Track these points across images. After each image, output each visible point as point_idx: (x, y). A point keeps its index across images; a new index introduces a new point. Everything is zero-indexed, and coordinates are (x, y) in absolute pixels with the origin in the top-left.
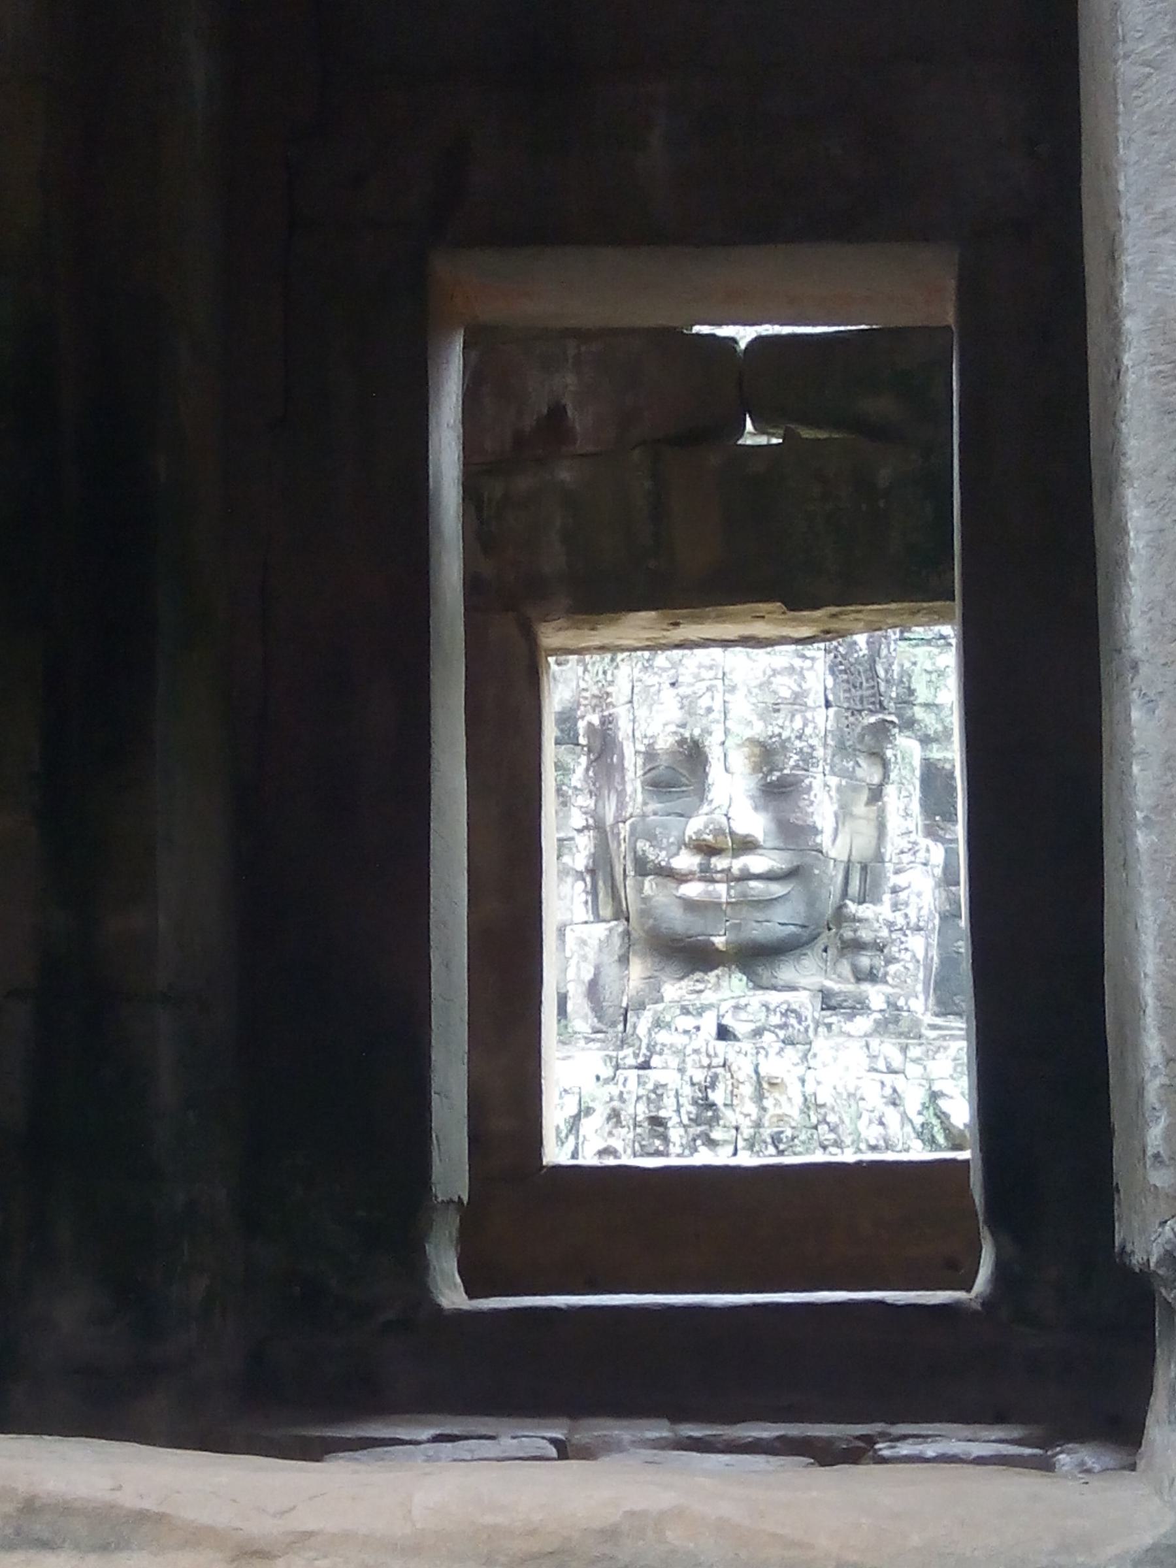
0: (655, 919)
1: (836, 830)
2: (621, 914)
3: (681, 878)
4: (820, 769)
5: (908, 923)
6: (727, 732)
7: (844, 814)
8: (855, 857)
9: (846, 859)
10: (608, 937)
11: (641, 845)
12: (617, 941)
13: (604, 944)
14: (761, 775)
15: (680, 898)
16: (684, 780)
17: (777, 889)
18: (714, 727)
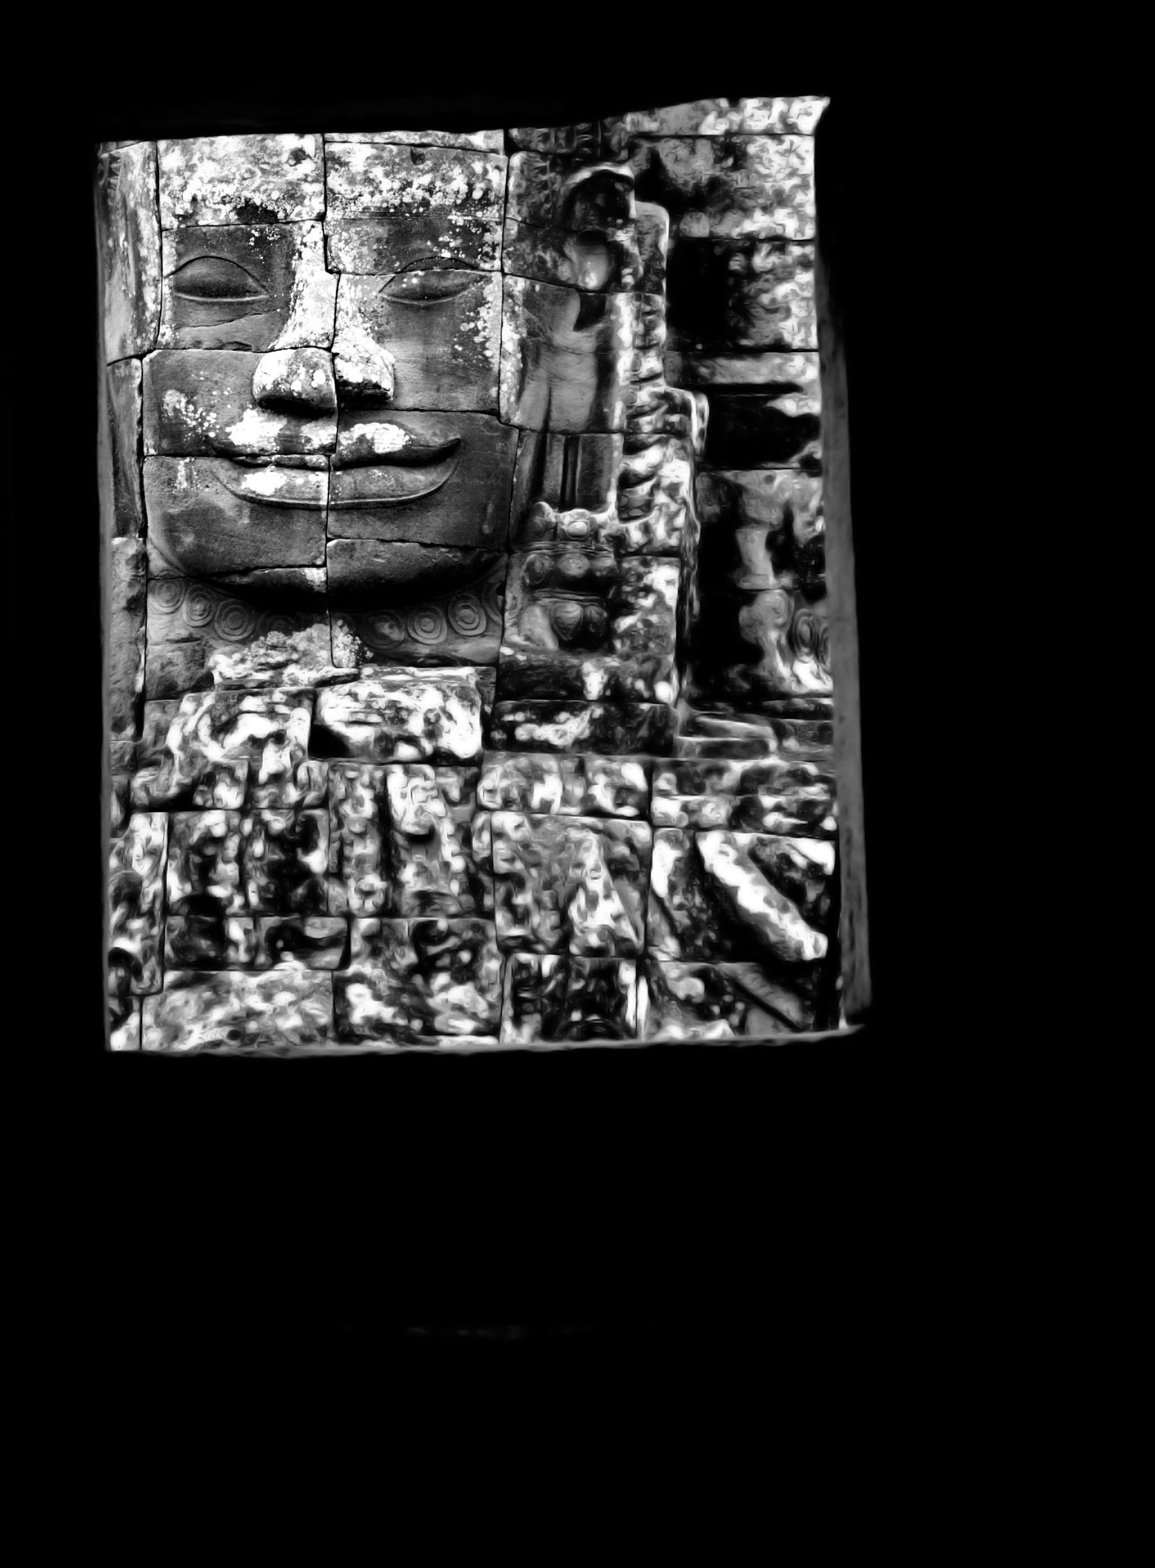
1: (523, 375)
3: (249, 461)
4: (497, 264)
6: (329, 196)
8: (557, 422)
9: (537, 423)
11: (173, 399)
15: (244, 498)
17: (419, 481)
18: (307, 188)
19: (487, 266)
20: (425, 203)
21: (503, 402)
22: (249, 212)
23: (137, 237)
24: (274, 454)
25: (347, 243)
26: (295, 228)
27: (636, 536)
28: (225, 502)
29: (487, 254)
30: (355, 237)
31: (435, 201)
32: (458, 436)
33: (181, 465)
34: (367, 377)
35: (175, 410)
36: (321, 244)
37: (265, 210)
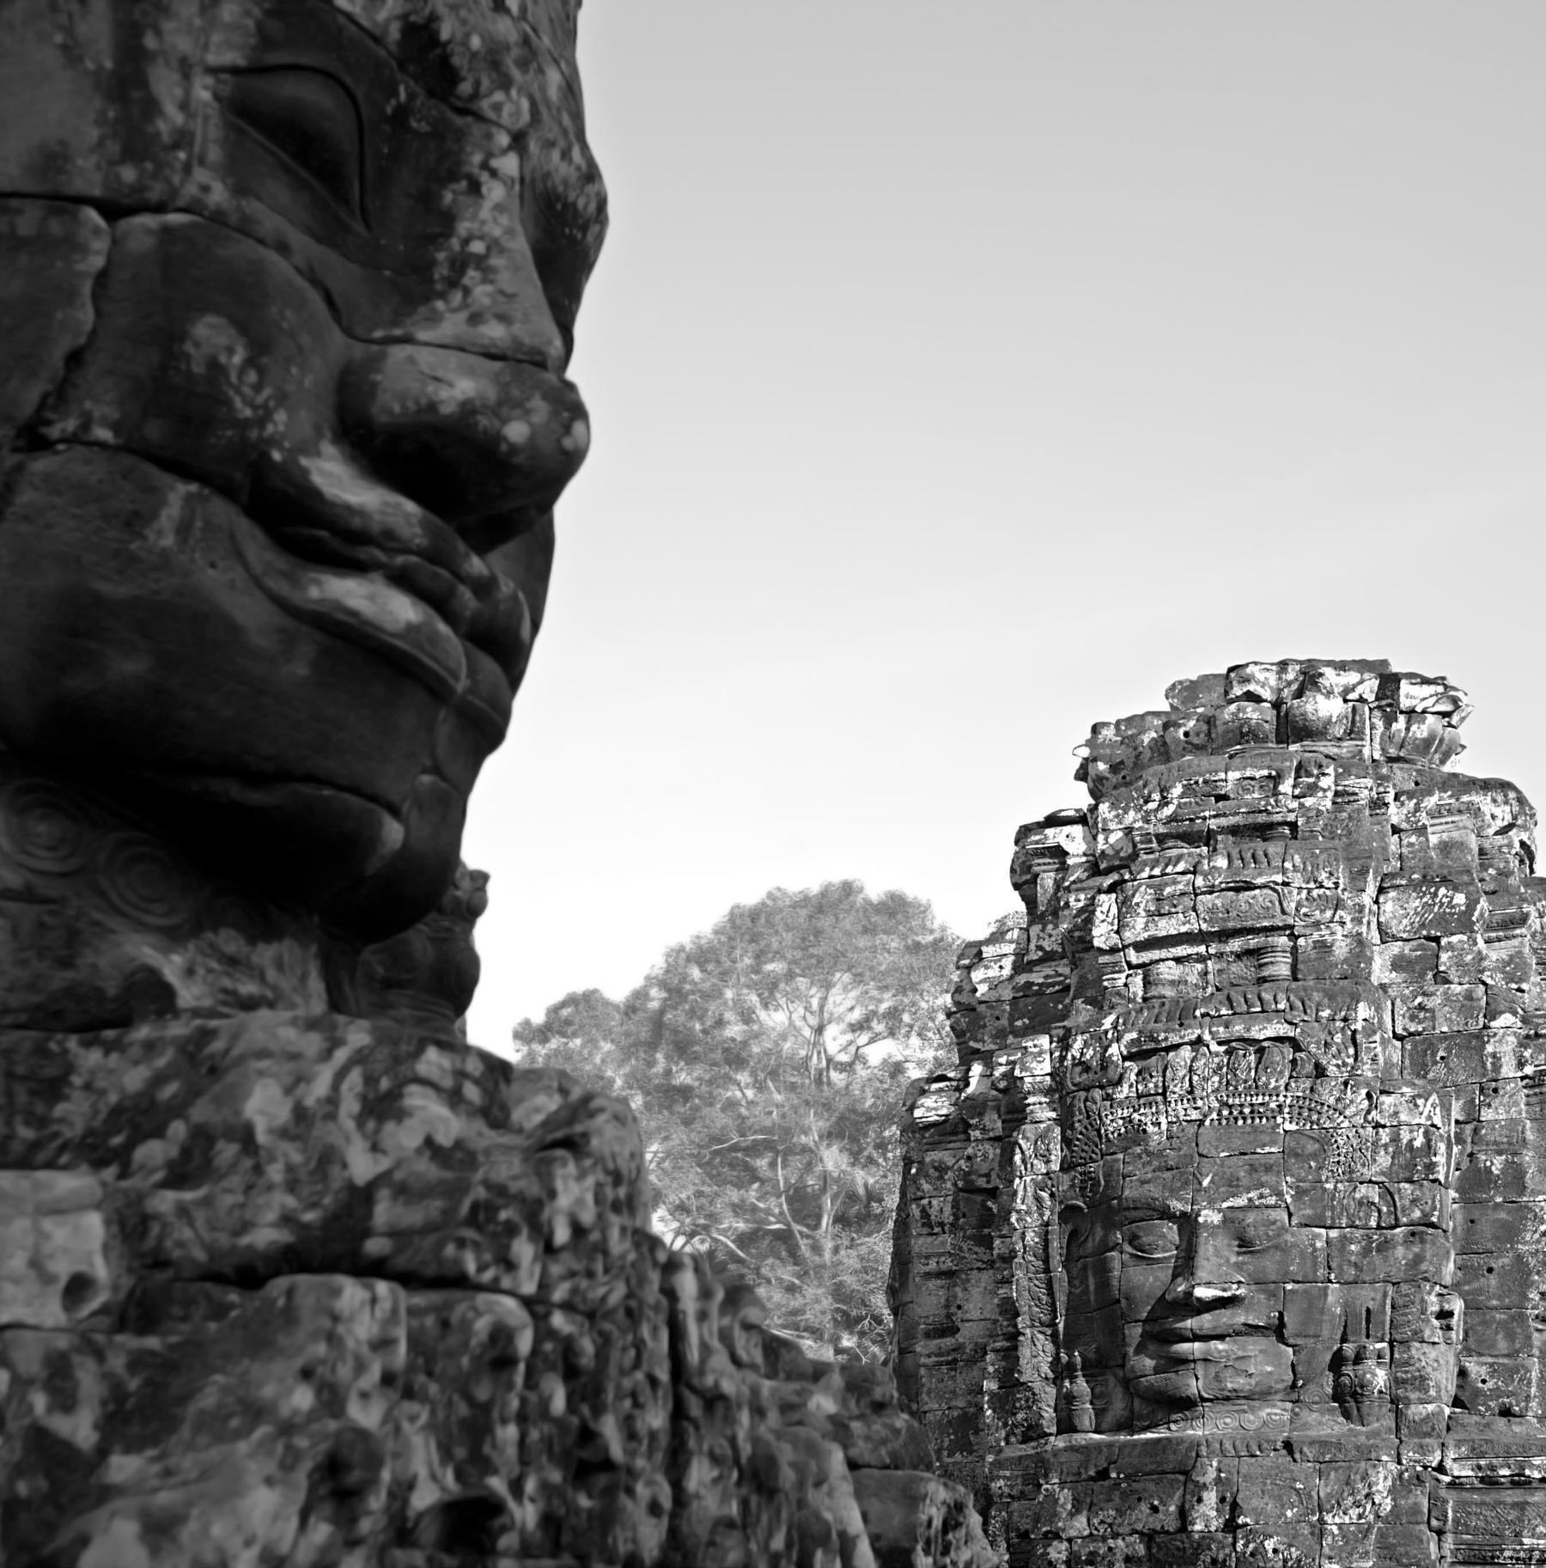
3: (341, 544)
11: (212, 337)
24: (407, 551)
26: (477, 130)
28: (250, 613)
33: (178, 492)
35: (214, 366)
37: (445, 61)
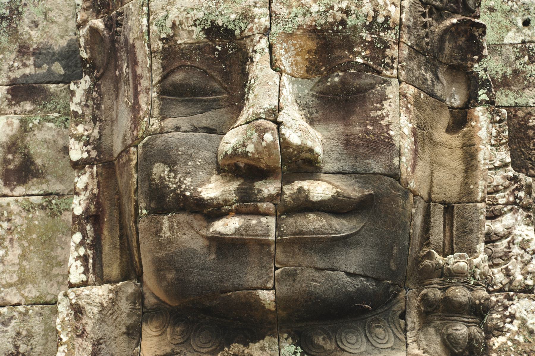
0: (177, 270)
2: (131, 271)
3: (213, 211)
5: (511, 282)
6: (273, 16)
7: (422, 135)
8: (437, 196)
10: (113, 302)
11: (159, 170)
12: (125, 306)
13: (107, 311)
14: (318, 78)
16: (216, 85)
18: (256, 11)
19: (388, 73)
20: (343, 22)
21: (403, 170)
22: (214, 31)
23: (134, 62)
24: (234, 203)
25: (286, 51)
26: (248, 41)
27: (499, 277)
29: (387, 64)
30: (292, 48)
31: (351, 21)
32: (372, 192)
33: (165, 220)
34: (305, 142)
35: (160, 177)
36: (267, 50)
37: (226, 29)
